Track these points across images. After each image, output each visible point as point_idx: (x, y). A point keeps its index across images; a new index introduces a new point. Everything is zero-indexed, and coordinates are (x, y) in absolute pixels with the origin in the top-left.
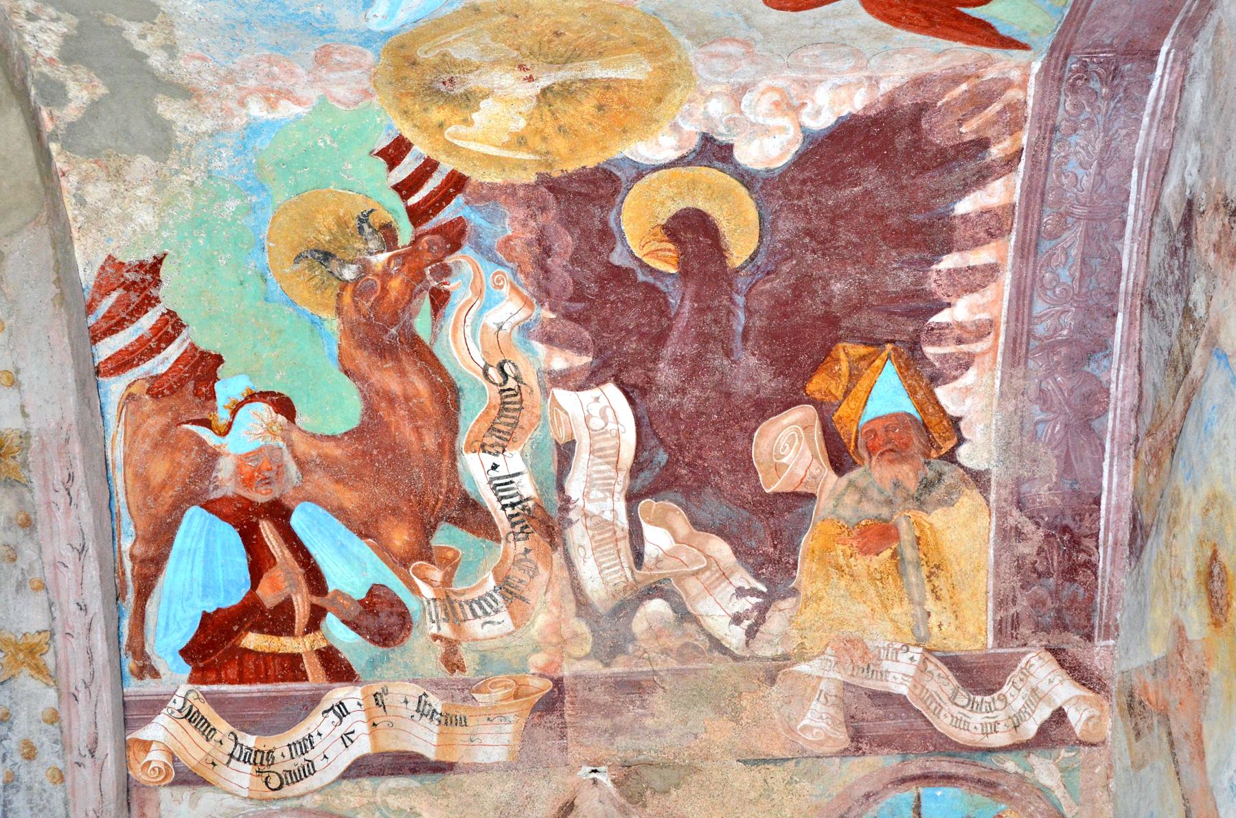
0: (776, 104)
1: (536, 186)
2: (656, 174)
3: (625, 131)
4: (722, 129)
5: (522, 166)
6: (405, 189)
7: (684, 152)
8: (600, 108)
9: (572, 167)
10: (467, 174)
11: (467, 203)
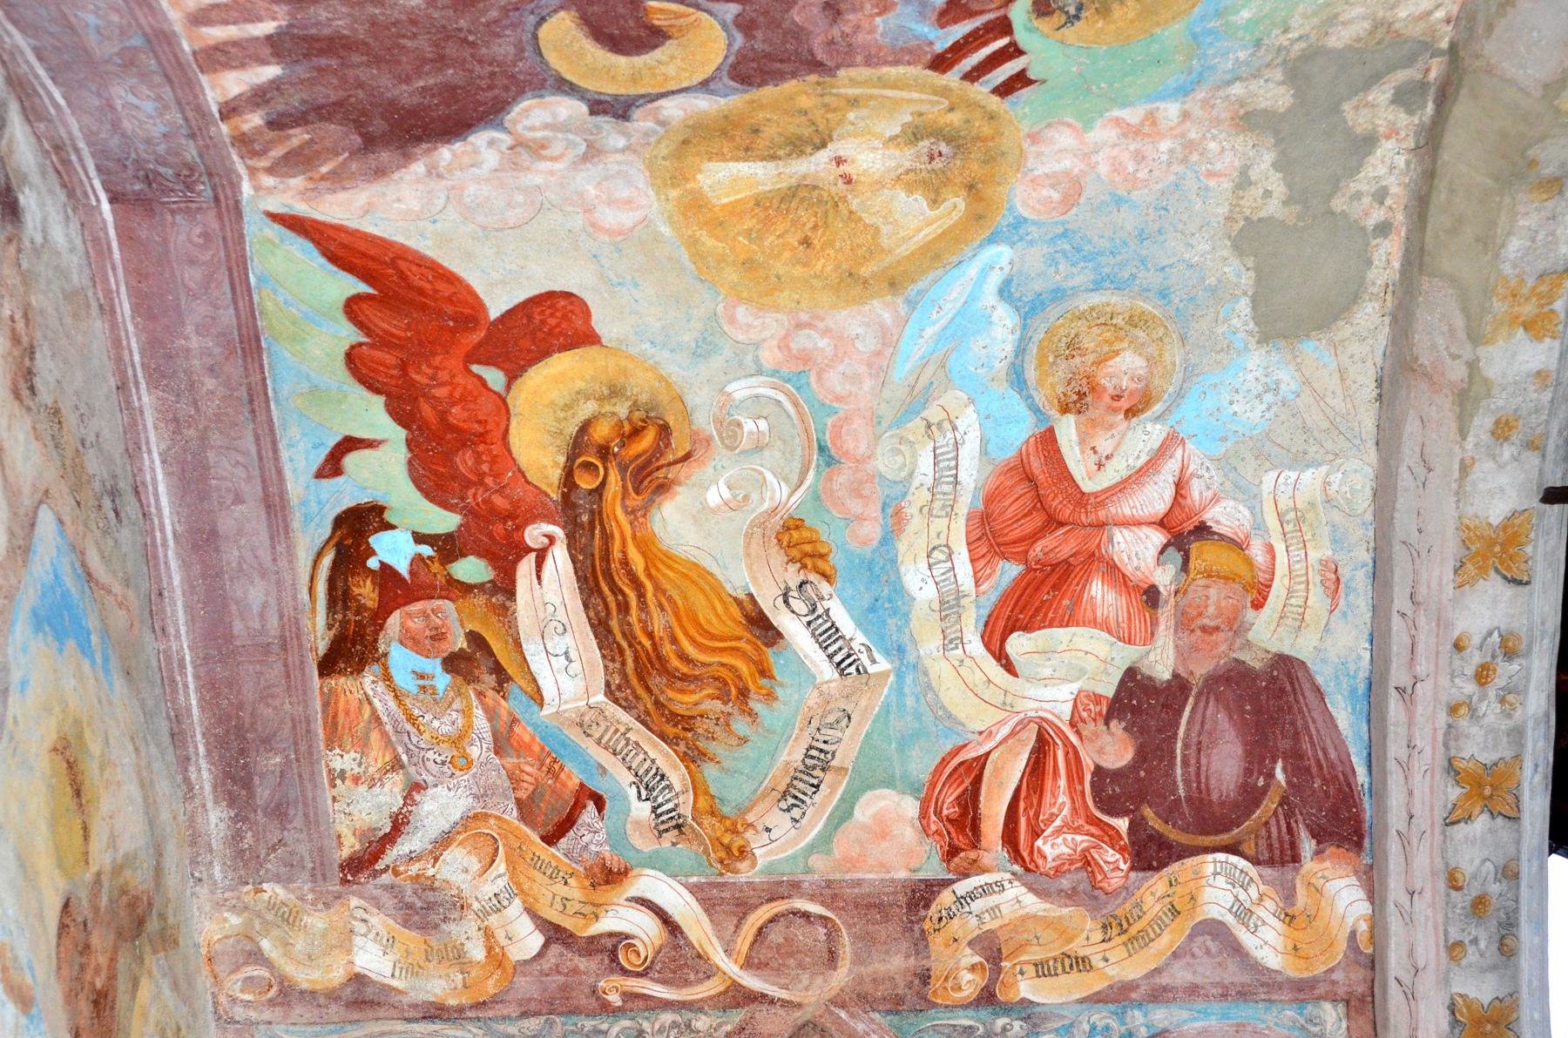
0: (543, 147)
1: (838, 67)
2: (685, 85)
3: (726, 117)
4: (606, 127)
5: (853, 82)
6: (1013, 51)
7: (650, 106)
8: (756, 131)
9: (790, 86)
10: (929, 72)
11: (931, 43)
